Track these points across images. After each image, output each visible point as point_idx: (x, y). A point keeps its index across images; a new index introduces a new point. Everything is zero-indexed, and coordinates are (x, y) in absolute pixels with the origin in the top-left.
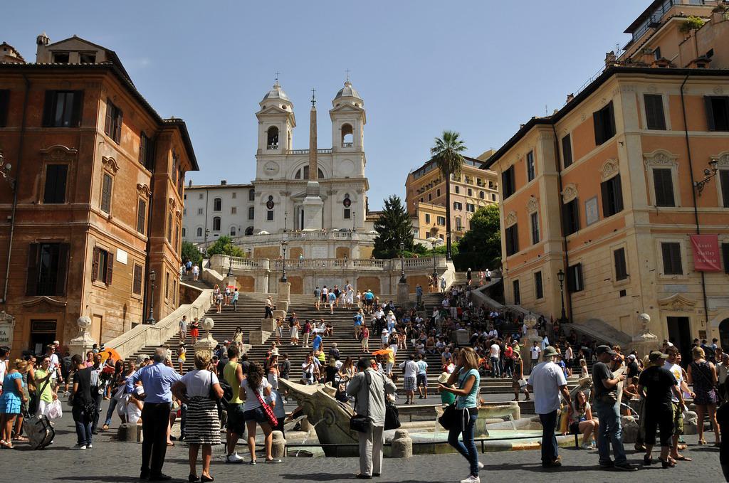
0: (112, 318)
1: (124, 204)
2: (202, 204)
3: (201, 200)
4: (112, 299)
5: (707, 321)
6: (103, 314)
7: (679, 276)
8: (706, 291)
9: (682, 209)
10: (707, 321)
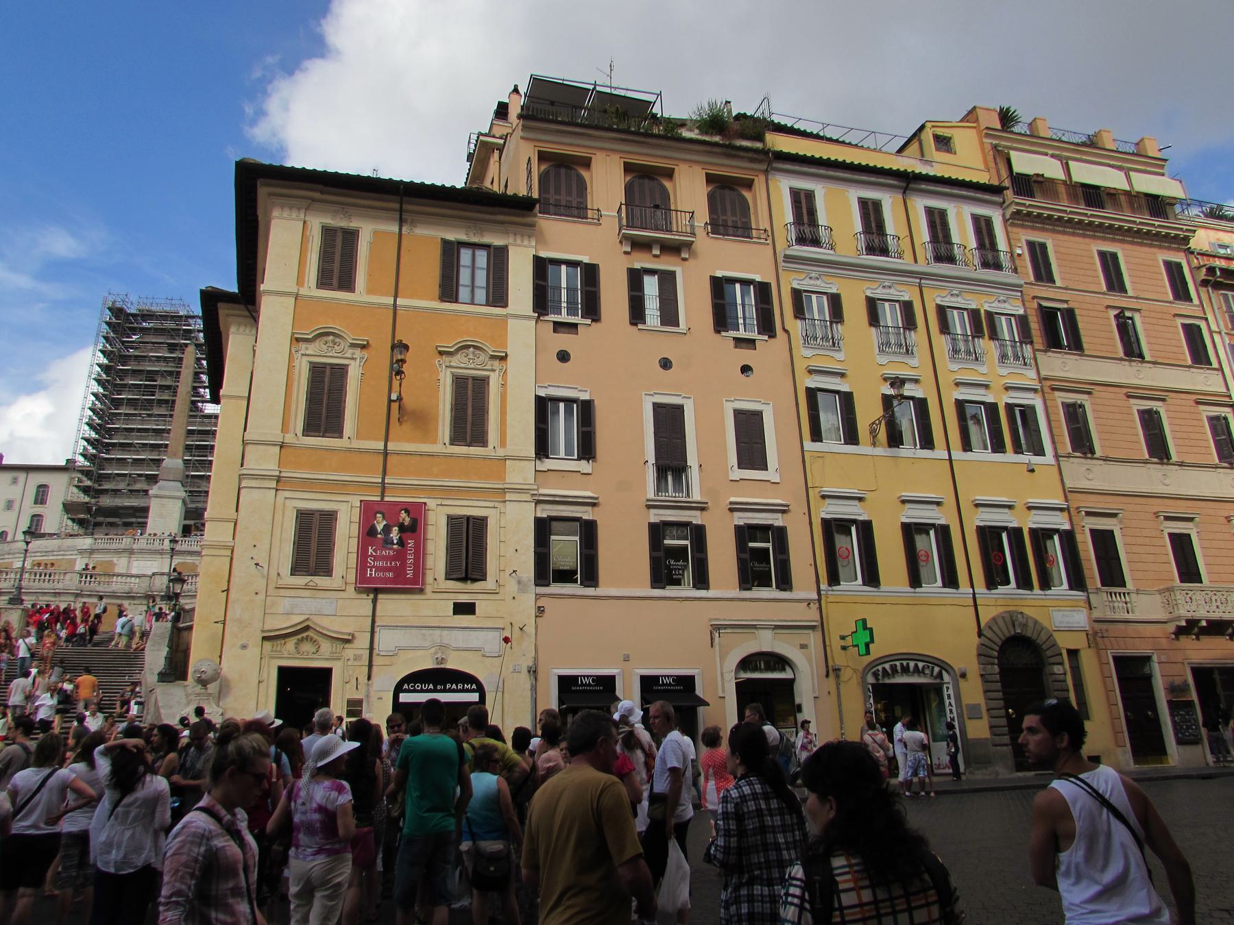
2: (15, 492)
3: (13, 487)
5: (369, 678)
7: (321, 581)
8: (378, 613)
9: (356, 444)
10: (369, 678)
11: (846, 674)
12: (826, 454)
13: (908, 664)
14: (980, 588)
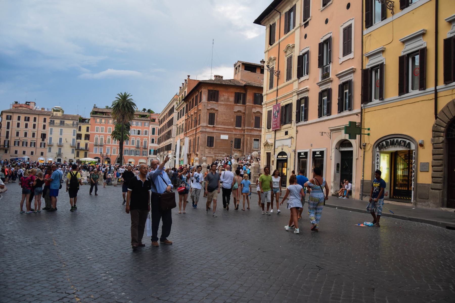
0: (219, 157)
1: (224, 120)
4: (219, 151)
6: (213, 156)
11: (368, 147)
12: (371, 33)
13: (394, 140)
14: (441, 85)
